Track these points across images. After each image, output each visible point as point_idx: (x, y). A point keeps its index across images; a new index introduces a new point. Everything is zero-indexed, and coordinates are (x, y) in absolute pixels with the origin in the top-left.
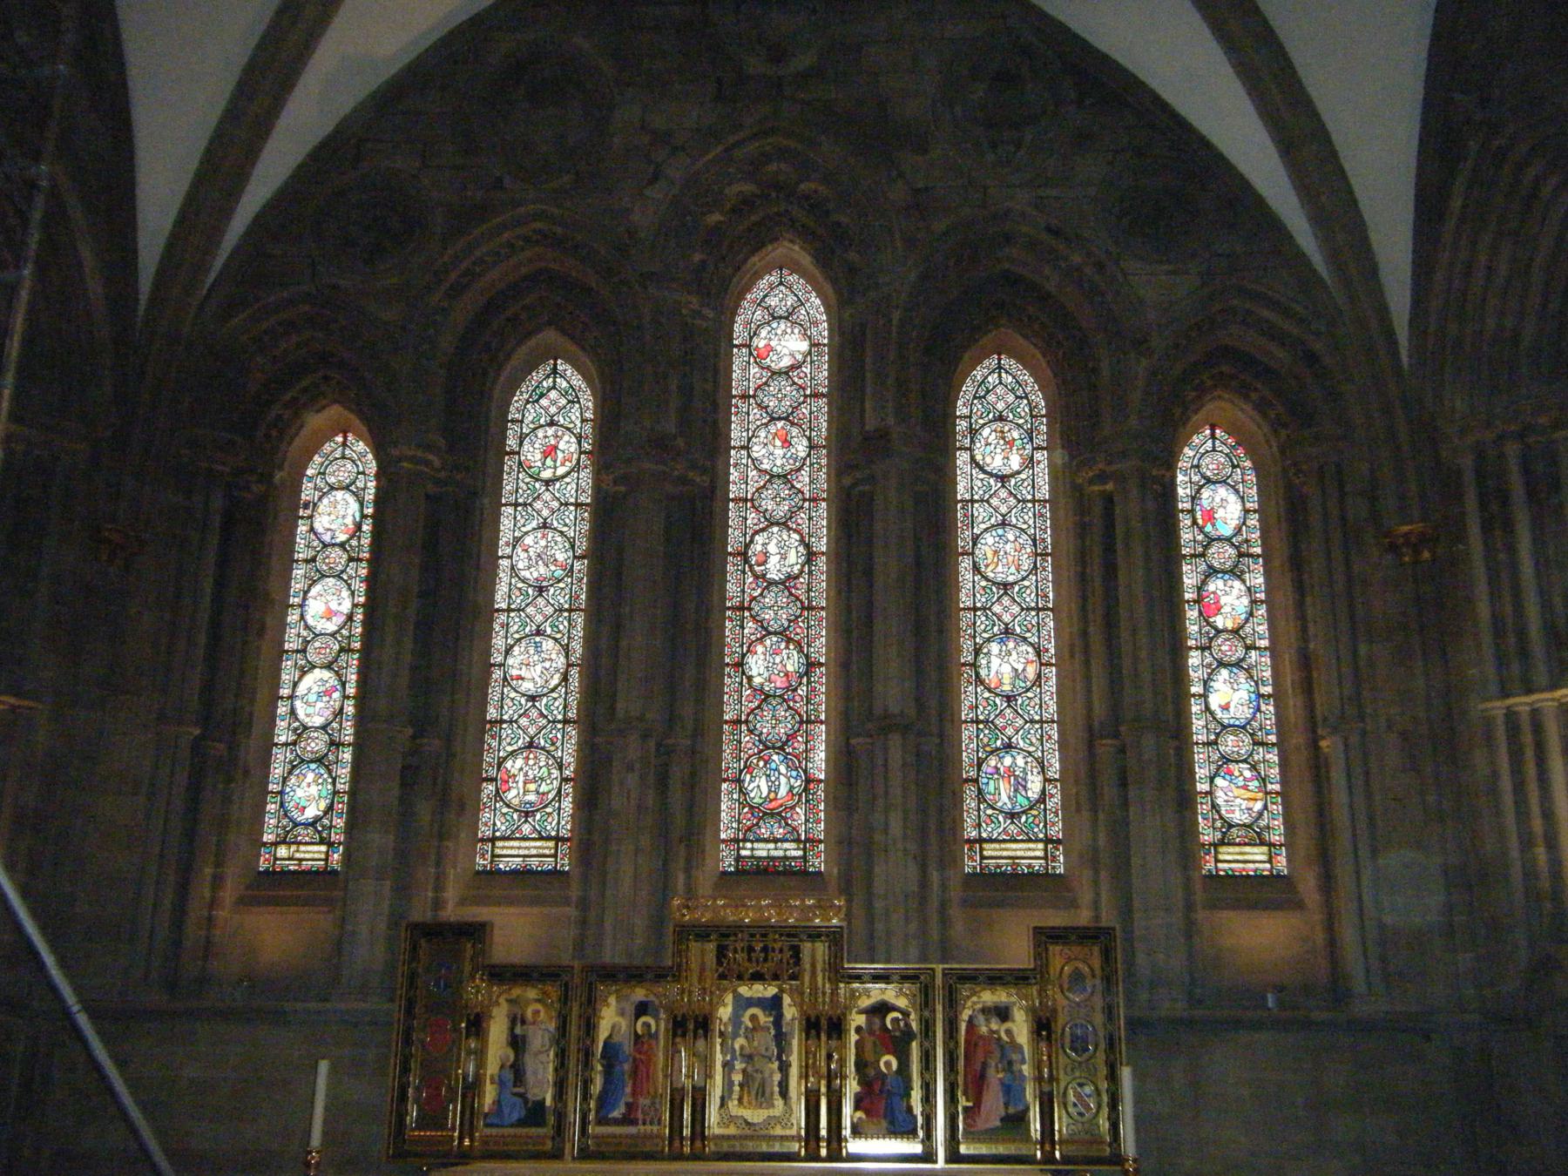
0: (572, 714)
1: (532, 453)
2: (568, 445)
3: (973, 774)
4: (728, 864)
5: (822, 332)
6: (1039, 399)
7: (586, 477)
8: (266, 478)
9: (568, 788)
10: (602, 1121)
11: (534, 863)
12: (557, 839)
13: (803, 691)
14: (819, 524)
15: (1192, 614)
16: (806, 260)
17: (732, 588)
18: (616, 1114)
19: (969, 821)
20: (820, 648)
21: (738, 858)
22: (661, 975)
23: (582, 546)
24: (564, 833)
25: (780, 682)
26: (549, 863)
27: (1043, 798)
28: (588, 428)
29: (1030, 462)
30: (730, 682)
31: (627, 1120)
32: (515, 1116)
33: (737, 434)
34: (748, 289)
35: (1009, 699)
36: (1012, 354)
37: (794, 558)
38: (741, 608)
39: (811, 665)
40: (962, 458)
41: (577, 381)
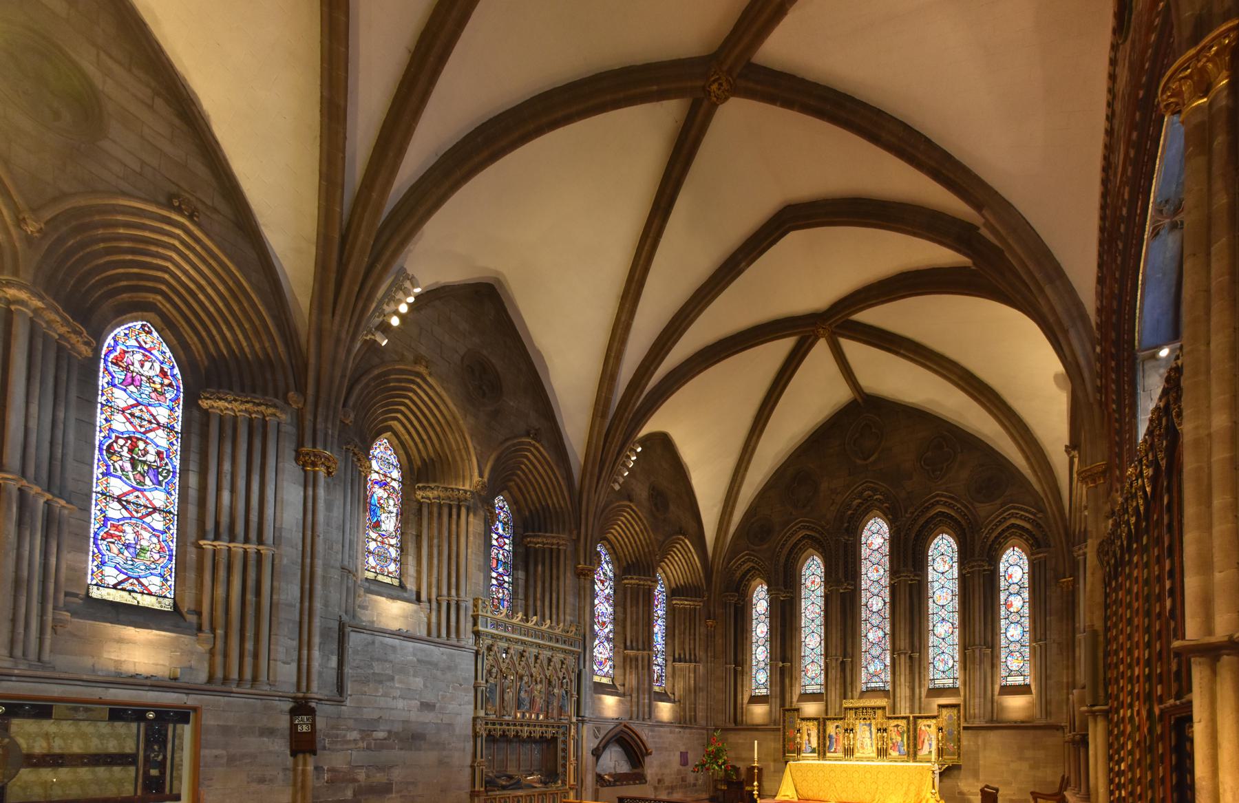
2: (818, 580)
6: (955, 547)
13: (883, 642)
16: (881, 514)
17: (863, 615)
19: (931, 674)
20: (888, 630)
23: (823, 608)
25: (877, 640)
27: (953, 666)
28: (823, 574)
30: (864, 641)
33: (864, 570)
36: (947, 533)
37: (881, 604)
39: (885, 634)
40: (930, 569)
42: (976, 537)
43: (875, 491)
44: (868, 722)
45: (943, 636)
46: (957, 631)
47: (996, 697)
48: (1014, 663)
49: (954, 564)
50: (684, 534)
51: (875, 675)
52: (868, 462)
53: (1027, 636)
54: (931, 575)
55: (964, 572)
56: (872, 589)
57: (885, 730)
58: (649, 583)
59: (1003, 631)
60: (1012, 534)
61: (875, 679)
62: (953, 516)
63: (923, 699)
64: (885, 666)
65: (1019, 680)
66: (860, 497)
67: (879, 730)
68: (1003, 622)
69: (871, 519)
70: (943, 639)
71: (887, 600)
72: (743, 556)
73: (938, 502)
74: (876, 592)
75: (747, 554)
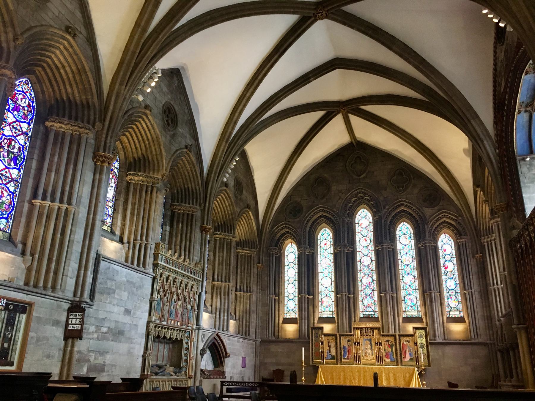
0: (333, 290)
1: (322, 245)
2: (328, 243)
3: (404, 299)
4: (362, 316)
5: (371, 220)
6: (411, 230)
7: (332, 248)
8: (280, 253)
9: (333, 303)
10: (344, 359)
11: (329, 316)
12: (332, 312)
13: (372, 285)
14: (373, 255)
15: (443, 269)
18: (346, 358)
19: (404, 307)
20: (375, 277)
21: (363, 315)
22: (351, 335)
23: (332, 261)
24: (333, 311)
26: (331, 316)
27: (417, 303)
28: (332, 240)
30: (360, 284)
31: (348, 359)
32: (330, 358)
33: (357, 240)
34: (357, 213)
35: (409, 285)
36: (406, 222)
38: (360, 271)
39: (373, 280)
40: (398, 242)
41: (329, 231)
42: (426, 227)
43: (365, 194)
44: (369, 338)
45: (409, 284)
46: (417, 281)
47: (445, 324)
48: (453, 303)
50: (249, 209)
52: (360, 177)
53: (458, 286)
54: (399, 246)
55: (419, 246)
56: (363, 252)
57: (381, 344)
58: (231, 238)
59: (444, 282)
61: (368, 309)
62: (410, 213)
63: (401, 324)
64: (374, 301)
65: (456, 314)
66: (356, 197)
67: (377, 344)
68: (443, 277)
69: (361, 209)
70: (409, 285)
71: (374, 259)
72: (282, 225)
73: (402, 204)
74: (366, 253)
75: (285, 224)
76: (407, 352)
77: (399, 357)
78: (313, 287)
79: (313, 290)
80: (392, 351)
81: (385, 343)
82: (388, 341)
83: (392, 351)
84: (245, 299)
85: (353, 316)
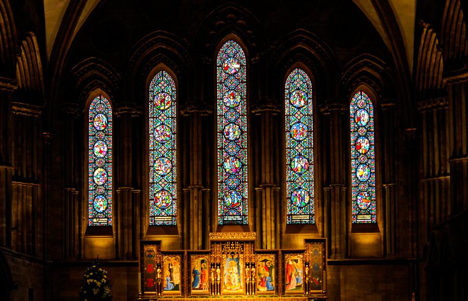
4: (221, 222)
20: (245, 160)
29: (306, 103)
36: (302, 69)
39: (243, 165)
49: (309, 101)
51: (233, 207)
60: (363, 80)
72: (86, 63)
75: (91, 61)
76: (293, 276)
77: (280, 285)
78: (141, 175)
79: (141, 179)
80: (270, 275)
81: (260, 263)
82: (265, 261)
83: (270, 275)
84: (25, 193)
85: (208, 222)
